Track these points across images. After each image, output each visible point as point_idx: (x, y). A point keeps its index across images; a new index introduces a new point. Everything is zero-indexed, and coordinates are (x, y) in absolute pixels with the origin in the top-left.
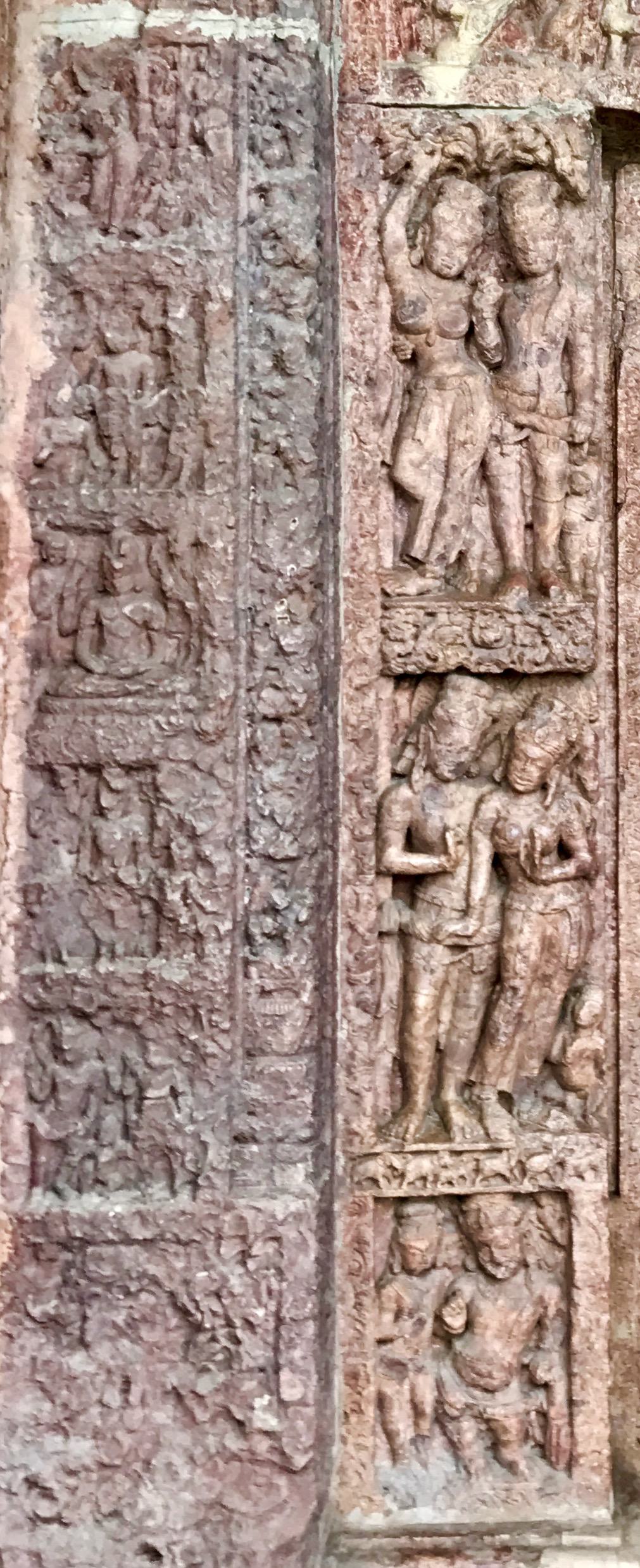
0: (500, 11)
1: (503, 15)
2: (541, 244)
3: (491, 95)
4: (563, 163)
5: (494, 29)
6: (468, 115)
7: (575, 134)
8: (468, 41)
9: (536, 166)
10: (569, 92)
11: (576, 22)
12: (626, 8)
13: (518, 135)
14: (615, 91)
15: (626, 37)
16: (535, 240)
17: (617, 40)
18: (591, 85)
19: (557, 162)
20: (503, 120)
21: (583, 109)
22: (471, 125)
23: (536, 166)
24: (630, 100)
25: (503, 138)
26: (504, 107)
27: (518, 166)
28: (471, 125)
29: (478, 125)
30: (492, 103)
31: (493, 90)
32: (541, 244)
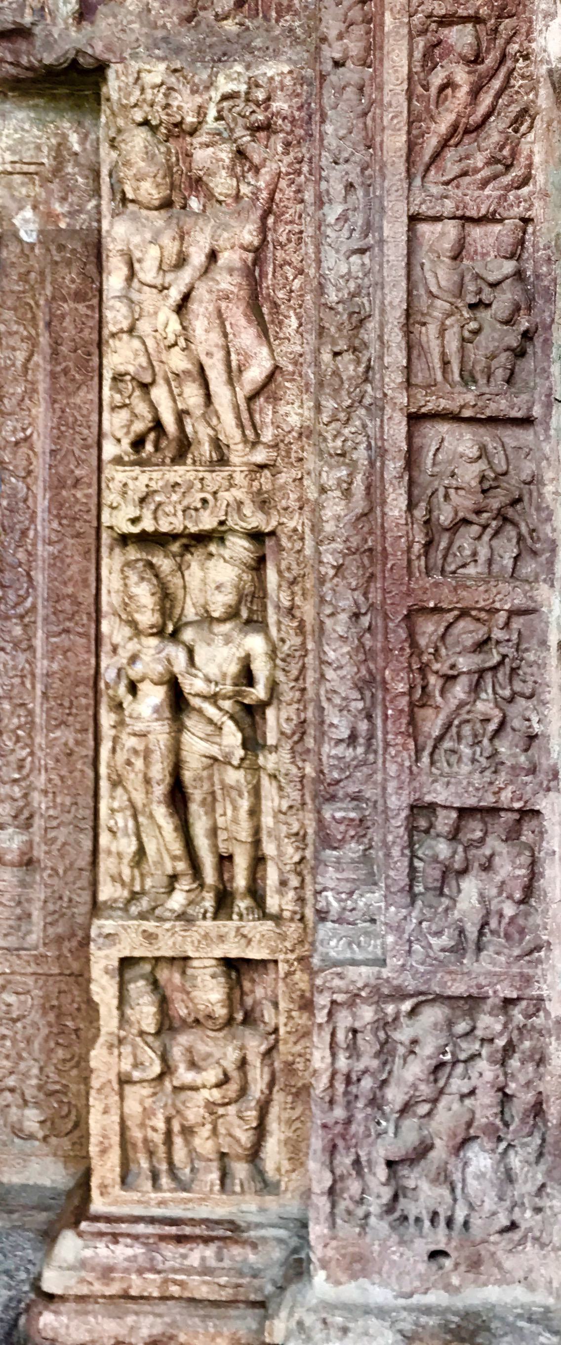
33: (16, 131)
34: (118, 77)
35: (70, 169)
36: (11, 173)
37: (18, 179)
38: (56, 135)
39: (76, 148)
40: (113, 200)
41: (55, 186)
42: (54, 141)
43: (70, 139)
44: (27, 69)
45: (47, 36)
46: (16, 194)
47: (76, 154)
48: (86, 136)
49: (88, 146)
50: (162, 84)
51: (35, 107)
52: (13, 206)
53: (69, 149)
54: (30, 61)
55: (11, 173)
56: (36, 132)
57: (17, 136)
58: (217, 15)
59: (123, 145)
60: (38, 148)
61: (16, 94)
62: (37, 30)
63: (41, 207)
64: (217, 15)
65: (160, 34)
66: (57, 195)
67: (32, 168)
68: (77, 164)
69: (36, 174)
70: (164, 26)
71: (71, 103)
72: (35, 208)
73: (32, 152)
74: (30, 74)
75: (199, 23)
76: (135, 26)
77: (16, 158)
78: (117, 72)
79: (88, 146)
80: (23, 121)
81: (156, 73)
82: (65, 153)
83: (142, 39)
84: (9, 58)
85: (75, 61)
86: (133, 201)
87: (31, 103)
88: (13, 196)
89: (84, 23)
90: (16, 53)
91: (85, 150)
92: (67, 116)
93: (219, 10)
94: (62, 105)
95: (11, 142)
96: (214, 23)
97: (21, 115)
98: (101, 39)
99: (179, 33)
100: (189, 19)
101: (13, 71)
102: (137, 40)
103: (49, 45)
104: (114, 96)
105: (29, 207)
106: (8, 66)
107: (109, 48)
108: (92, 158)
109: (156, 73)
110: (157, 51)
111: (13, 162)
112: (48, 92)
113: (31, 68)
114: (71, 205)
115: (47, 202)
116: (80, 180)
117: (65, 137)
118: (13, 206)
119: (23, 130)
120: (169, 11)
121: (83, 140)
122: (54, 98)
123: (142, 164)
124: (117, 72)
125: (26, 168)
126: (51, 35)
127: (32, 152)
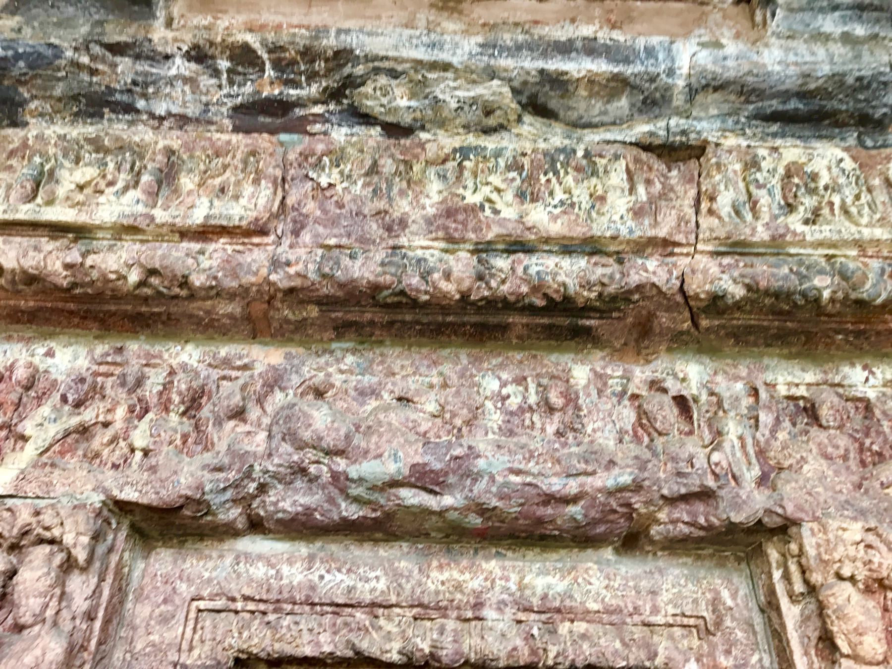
0: (57, 433)
1: (59, 436)
2: (32, 601)
3: (31, 489)
4: (68, 539)
5: (51, 446)
6: (10, 502)
7: (81, 517)
8: (30, 451)
9: (52, 542)
10: (89, 487)
11: (111, 442)
12: (148, 433)
13: (41, 517)
14: (127, 489)
15: (146, 453)
16: (27, 598)
17: (139, 455)
18: (108, 484)
19: (65, 537)
20: (35, 505)
21: (97, 499)
22: (9, 510)
23: (52, 542)
24: (137, 494)
25: (33, 520)
26: (38, 497)
27: (41, 541)
28: (9, 510)
29: (15, 509)
30: (30, 495)
31: (33, 484)
32: (32, 601)
33: (673, 586)
34: (813, 534)
35: (728, 622)
36: (671, 626)
37: (677, 631)
38: (710, 590)
39: (730, 603)
40: (806, 653)
41: (717, 639)
42: (709, 596)
43: (722, 594)
44: (702, 528)
45: (733, 497)
46: (680, 646)
47: (731, 609)
48: (737, 592)
49: (739, 601)
50: (862, 541)
51: (685, 564)
52: (679, 658)
53: (724, 604)
54: (707, 520)
55: (671, 626)
56: (690, 585)
57: (675, 590)
58: (882, 484)
59: (832, 600)
60: (695, 601)
61: (666, 553)
62: (722, 493)
63: (705, 660)
64: (882, 484)
65: (843, 498)
66: (721, 648)
67: (692, 621)
68: (733, 619)
69: (695, 626)
70: (841, 491)
71: (714, 562)
72: (698, 660)
73: (690, 606)
74: (702, 533)
75: (867, 492)
76: (820, 489)
77: (678, 611)
78: (812, 530)
79: (739, 601)
80: (677, 576)
81: (855, 531)
82: (721, 607)
83: (830, 501)
84: (686, 518)
85: (760, 522)
86: (848, 656)
87: (680, 561)
88: (677, 648)
89: (762, 488)
90: (695, 515)
91: (737, 605)
92: (717, 573)
93: (885, 480)
94: (707, 563)
95: (671, 596)
96: (880, 491)
97: (677, 572)
98: (790, 500)
99: (855, 498)
100: (860, 486)
101: (686, 530)
102: (826, 502)
103: (737, 506)
104: (811, 551)
105: (693, 659)
106: (681, 525)
107: (800, 508)
108: (745, 612)
109: (855, 531)
110: (846, 513)
111: (674, 615)
112: (693, 552)
113: (709, 528)
114: (736, 658)
115: (712, 655)
116: (740, 634)
117: (717, 593)
118: (679, 658)
119: (680, 585)
120: (843, 479)
121: (734, 596)
122: (699, 557)
123: (862, 618)
124: (812, 530)
125: (686, 621)
126: (738, 495)
127: (690, 606)
